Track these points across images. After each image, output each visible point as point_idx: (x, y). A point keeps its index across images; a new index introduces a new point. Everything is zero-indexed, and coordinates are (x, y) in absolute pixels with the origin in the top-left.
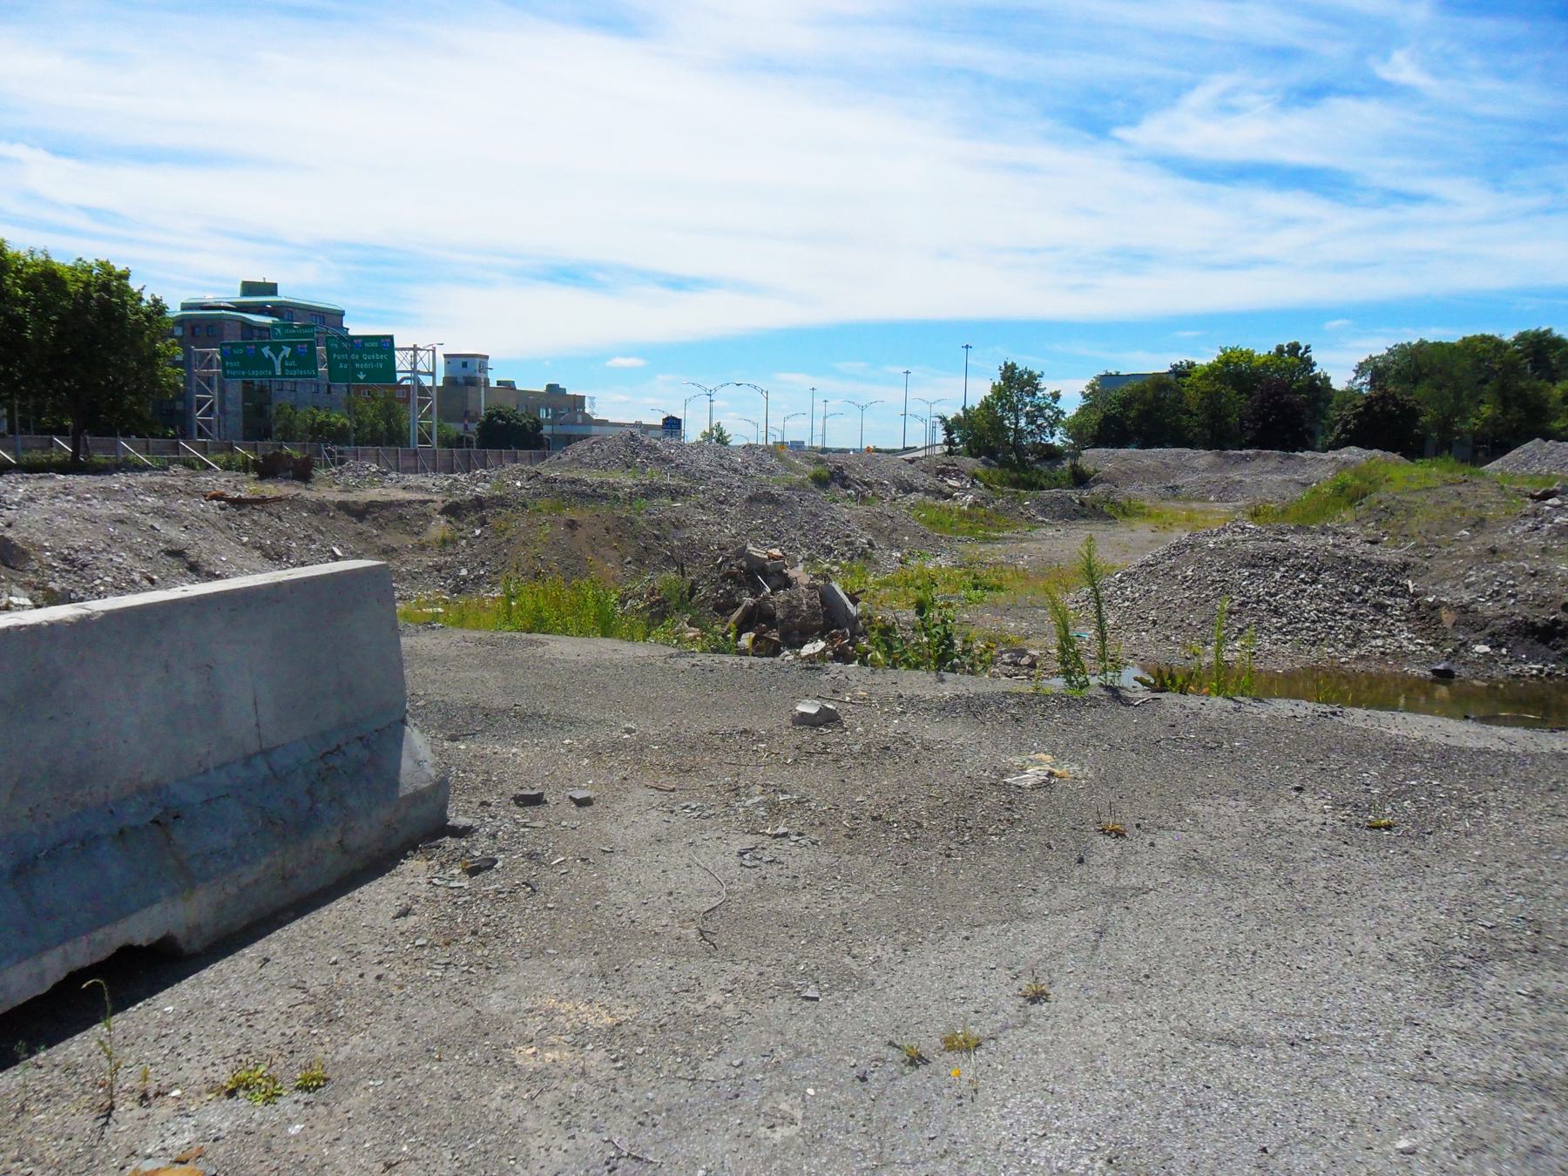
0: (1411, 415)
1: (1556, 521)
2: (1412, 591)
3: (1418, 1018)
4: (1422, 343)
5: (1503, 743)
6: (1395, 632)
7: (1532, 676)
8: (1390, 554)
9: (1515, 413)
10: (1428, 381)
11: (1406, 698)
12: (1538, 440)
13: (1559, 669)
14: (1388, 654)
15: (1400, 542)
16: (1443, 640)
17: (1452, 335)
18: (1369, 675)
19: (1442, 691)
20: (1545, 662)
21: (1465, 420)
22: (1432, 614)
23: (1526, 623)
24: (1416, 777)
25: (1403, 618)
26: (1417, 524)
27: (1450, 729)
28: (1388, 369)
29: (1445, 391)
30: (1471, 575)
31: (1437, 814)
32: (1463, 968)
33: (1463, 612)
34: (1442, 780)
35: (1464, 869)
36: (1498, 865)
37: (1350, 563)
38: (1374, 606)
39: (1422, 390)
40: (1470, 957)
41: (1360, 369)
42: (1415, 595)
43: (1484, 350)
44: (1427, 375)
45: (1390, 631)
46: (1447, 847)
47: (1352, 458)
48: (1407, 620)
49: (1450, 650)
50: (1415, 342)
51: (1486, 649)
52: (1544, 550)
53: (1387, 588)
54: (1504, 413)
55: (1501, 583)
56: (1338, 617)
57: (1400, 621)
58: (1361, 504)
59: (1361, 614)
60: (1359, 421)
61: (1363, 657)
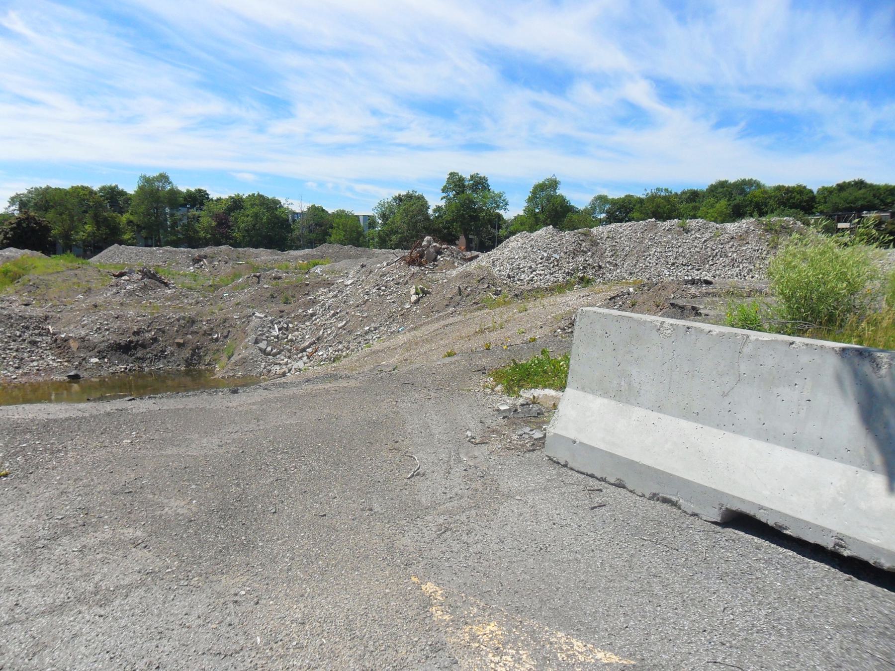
0: (47, 229)
1: (127, 288)
2: (51, 332)
3: (13, 586)
4: (48, 188)
5: (80, 412)
6: (44, 357)
7: (122, 372)
8: (36, 311)
9: (104, 230)
10: (53, 210)
11: (56, 394)
12: (116, 245)
13: (135, 366)
14: (41, 370)
15: (43, 304)
16: (73, 358)
17: (65, 184)
18: (31, 384)
19: (75, 387)
20: (127, 363)
21: (77, 233)
22: (65, 344)
23: (116, 344)
24: (27, 441)
25: (48, 348)
26: (53, 293)
27: (50, 410)
28: (29, 202)
29: (64, 216)
30: (84, 320)
31: (37, 461)
32: (43, 547)
33: (82, 341)
34: (42, 440)
35: (49, 489)
36: (69, 482)
37: (12, 318)
38: (30, 342)
39: (50, 215)
40: (48, 539)
41: (13, 201)
42: (54, 334)
43: (84, 194)
44: (53, 207)
45: (41, 356)
46: (41, 479)
47: (12, 254)
48: (50, 349)
49: (77, 363)
50: (44, 186)
51: (97, 360)
52: (122, 304)
53: (37, 332)
54: (98, 229)
55: (101, 323)
56: (8, 351)
57: (46, 350)
58: (18, 282)
59: (22, 348)
60: (14, 232)
61: (26, 374)
